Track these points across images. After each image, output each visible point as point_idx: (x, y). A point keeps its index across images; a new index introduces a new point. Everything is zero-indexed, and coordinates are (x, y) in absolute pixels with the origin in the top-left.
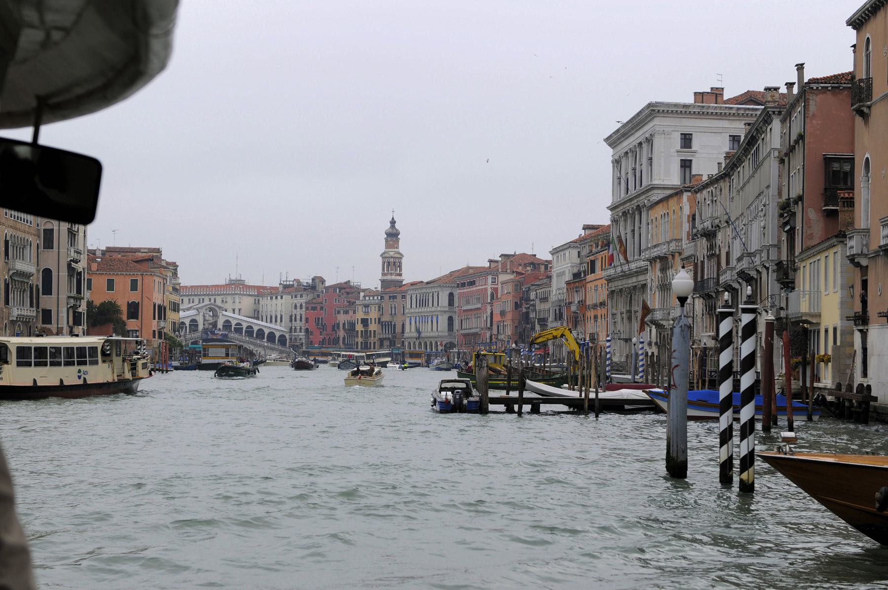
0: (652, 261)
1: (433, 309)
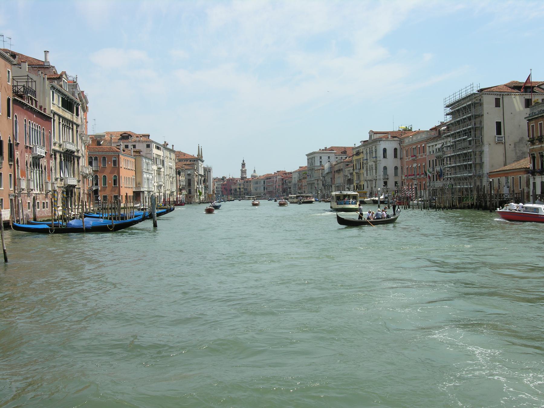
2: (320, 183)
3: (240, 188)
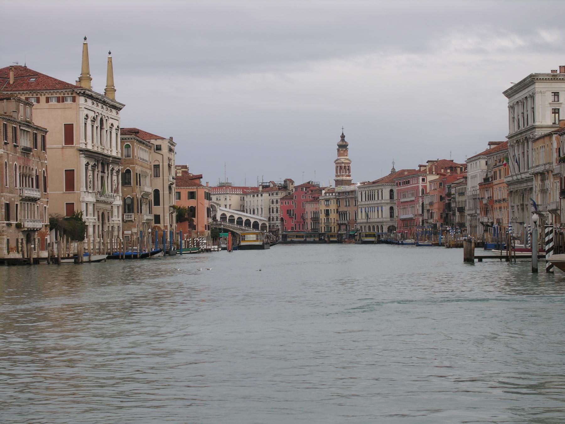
0: (536, 174)
1: (379, 202)
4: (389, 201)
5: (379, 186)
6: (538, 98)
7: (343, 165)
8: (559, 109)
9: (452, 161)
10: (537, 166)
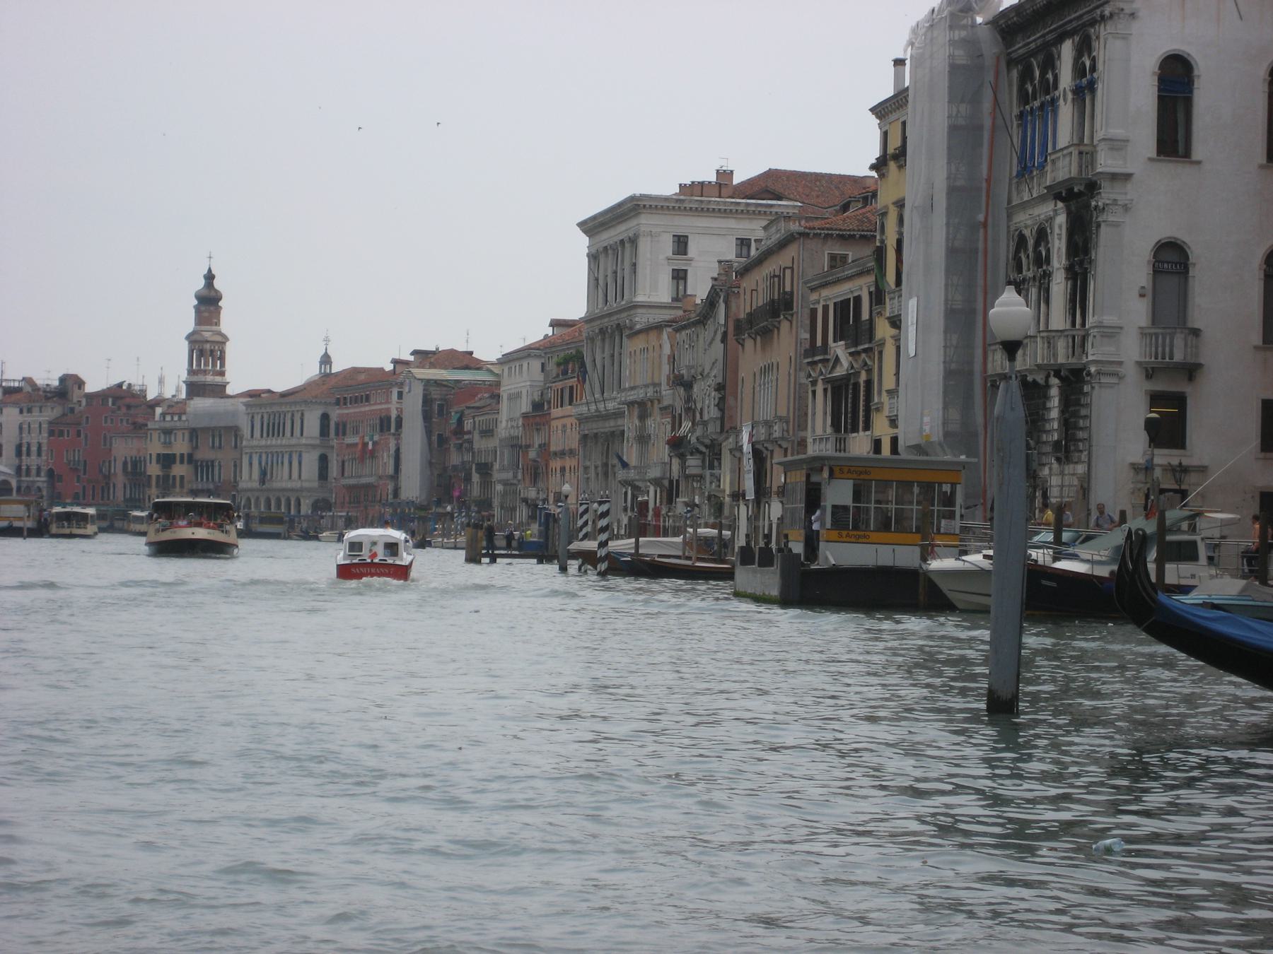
0: (631, 404)
1: (294, 441)
2: (659, 427)
3: (167, 461)
4: (318, 442)
5: (295, 403)
6: (644, 245)
7: (208, 346)
8: (686, 271)
9: (471, 353)
10: (632, 388)
